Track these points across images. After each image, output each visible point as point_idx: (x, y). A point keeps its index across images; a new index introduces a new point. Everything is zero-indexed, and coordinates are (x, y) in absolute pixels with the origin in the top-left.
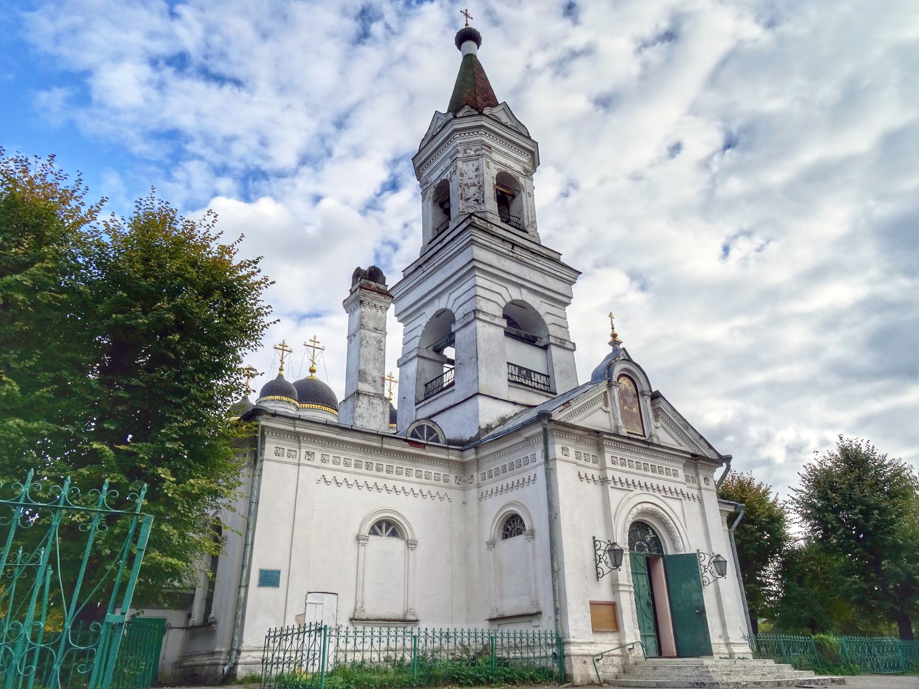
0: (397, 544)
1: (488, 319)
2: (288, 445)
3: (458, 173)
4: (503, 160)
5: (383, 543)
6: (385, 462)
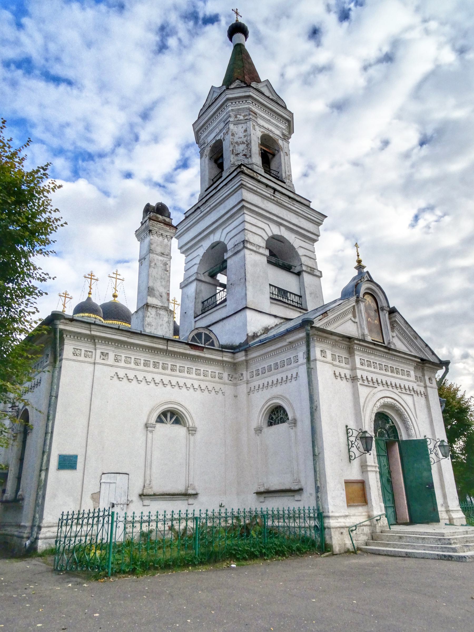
0: (180, 430)
1: (254, 249)
2: (85, 346)
3: (230, 133)
4: (266, 125)
5: (168, 429)
6: (170, 362)
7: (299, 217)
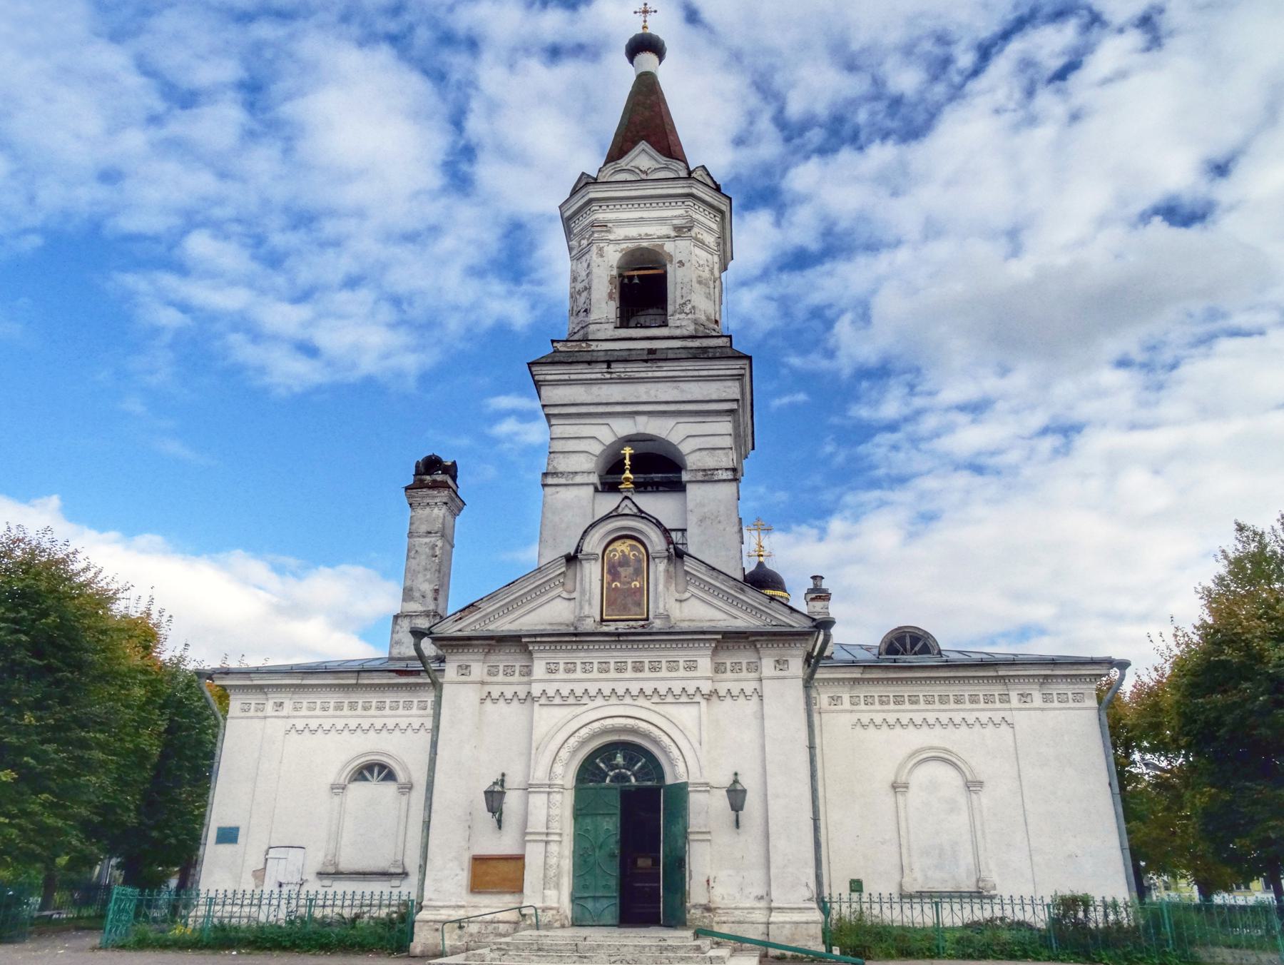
0: (390, 789)
1: (562, 481)
2: (253, 699)
5: (374, 789)
6: (374, 699)
7: (681, 384)
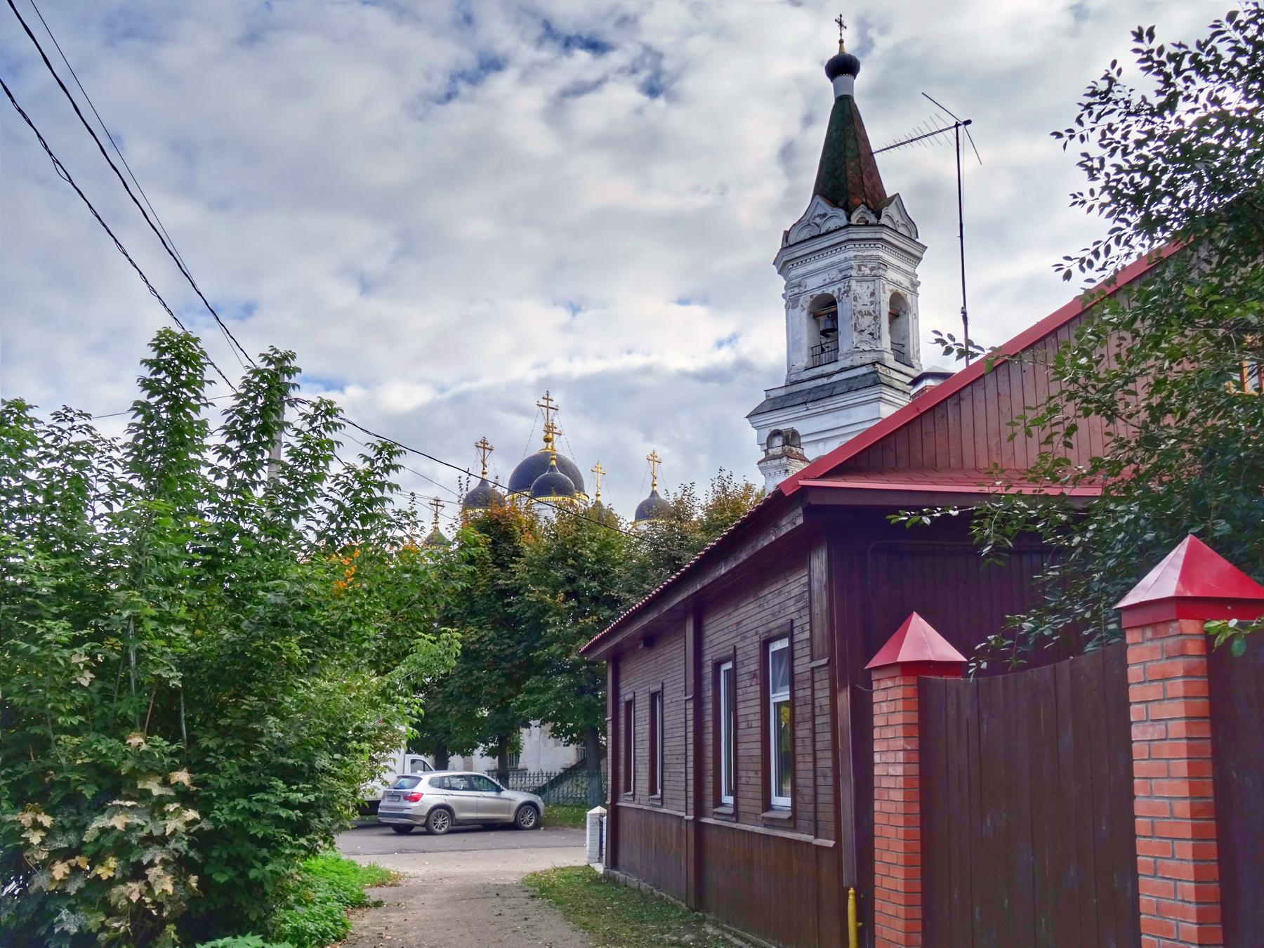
3: (852, 296)
